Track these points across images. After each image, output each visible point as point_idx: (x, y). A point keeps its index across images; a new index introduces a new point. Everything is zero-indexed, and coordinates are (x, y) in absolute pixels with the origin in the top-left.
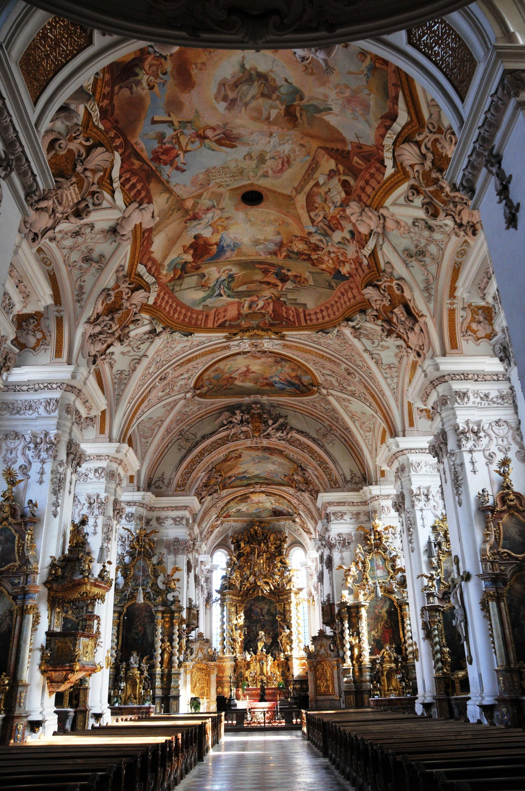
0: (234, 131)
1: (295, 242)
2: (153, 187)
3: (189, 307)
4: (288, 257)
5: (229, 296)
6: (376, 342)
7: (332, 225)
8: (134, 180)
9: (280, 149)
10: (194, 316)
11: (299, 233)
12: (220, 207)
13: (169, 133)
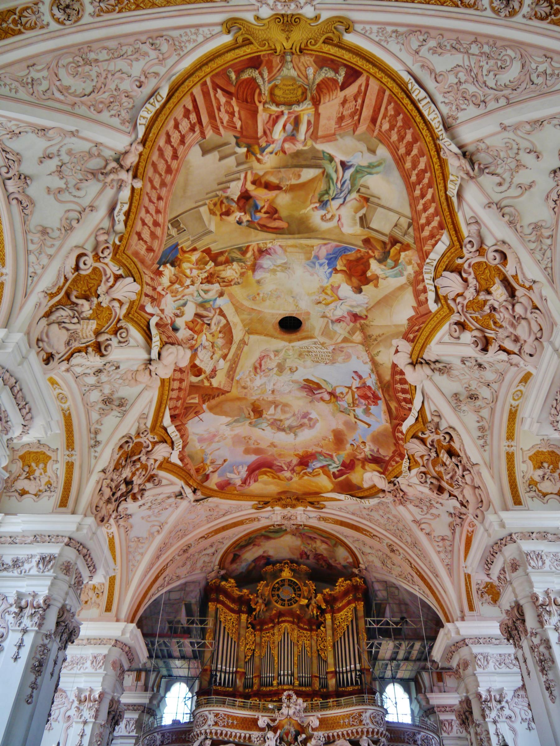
0: (305, 394)
1: (238, 276)
2: (387, 377)
3: (397, 164)
4: (244, 251)
5: (331, 159)
6: (66, 158)
7: (199, 322)
8: (401, 396)
9: (264, 380)
10: (394, 137)
11: (235, 290)
12: (326, 319)
13: (359, 411)
